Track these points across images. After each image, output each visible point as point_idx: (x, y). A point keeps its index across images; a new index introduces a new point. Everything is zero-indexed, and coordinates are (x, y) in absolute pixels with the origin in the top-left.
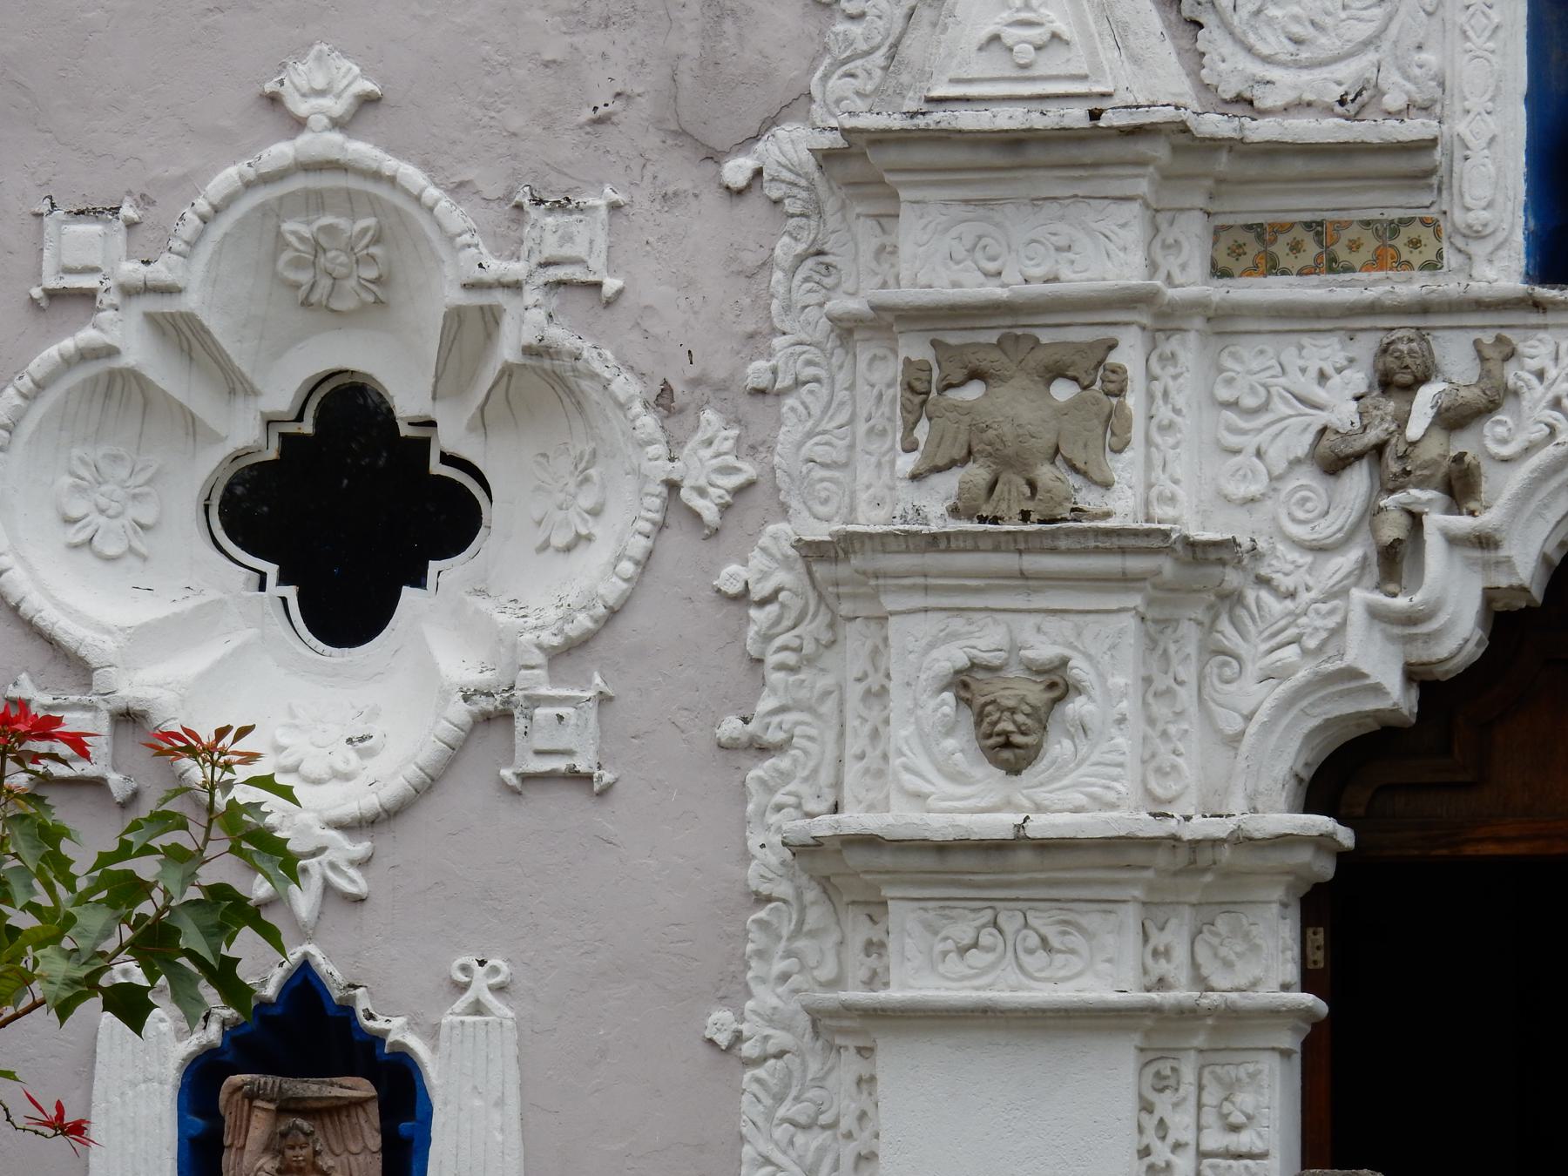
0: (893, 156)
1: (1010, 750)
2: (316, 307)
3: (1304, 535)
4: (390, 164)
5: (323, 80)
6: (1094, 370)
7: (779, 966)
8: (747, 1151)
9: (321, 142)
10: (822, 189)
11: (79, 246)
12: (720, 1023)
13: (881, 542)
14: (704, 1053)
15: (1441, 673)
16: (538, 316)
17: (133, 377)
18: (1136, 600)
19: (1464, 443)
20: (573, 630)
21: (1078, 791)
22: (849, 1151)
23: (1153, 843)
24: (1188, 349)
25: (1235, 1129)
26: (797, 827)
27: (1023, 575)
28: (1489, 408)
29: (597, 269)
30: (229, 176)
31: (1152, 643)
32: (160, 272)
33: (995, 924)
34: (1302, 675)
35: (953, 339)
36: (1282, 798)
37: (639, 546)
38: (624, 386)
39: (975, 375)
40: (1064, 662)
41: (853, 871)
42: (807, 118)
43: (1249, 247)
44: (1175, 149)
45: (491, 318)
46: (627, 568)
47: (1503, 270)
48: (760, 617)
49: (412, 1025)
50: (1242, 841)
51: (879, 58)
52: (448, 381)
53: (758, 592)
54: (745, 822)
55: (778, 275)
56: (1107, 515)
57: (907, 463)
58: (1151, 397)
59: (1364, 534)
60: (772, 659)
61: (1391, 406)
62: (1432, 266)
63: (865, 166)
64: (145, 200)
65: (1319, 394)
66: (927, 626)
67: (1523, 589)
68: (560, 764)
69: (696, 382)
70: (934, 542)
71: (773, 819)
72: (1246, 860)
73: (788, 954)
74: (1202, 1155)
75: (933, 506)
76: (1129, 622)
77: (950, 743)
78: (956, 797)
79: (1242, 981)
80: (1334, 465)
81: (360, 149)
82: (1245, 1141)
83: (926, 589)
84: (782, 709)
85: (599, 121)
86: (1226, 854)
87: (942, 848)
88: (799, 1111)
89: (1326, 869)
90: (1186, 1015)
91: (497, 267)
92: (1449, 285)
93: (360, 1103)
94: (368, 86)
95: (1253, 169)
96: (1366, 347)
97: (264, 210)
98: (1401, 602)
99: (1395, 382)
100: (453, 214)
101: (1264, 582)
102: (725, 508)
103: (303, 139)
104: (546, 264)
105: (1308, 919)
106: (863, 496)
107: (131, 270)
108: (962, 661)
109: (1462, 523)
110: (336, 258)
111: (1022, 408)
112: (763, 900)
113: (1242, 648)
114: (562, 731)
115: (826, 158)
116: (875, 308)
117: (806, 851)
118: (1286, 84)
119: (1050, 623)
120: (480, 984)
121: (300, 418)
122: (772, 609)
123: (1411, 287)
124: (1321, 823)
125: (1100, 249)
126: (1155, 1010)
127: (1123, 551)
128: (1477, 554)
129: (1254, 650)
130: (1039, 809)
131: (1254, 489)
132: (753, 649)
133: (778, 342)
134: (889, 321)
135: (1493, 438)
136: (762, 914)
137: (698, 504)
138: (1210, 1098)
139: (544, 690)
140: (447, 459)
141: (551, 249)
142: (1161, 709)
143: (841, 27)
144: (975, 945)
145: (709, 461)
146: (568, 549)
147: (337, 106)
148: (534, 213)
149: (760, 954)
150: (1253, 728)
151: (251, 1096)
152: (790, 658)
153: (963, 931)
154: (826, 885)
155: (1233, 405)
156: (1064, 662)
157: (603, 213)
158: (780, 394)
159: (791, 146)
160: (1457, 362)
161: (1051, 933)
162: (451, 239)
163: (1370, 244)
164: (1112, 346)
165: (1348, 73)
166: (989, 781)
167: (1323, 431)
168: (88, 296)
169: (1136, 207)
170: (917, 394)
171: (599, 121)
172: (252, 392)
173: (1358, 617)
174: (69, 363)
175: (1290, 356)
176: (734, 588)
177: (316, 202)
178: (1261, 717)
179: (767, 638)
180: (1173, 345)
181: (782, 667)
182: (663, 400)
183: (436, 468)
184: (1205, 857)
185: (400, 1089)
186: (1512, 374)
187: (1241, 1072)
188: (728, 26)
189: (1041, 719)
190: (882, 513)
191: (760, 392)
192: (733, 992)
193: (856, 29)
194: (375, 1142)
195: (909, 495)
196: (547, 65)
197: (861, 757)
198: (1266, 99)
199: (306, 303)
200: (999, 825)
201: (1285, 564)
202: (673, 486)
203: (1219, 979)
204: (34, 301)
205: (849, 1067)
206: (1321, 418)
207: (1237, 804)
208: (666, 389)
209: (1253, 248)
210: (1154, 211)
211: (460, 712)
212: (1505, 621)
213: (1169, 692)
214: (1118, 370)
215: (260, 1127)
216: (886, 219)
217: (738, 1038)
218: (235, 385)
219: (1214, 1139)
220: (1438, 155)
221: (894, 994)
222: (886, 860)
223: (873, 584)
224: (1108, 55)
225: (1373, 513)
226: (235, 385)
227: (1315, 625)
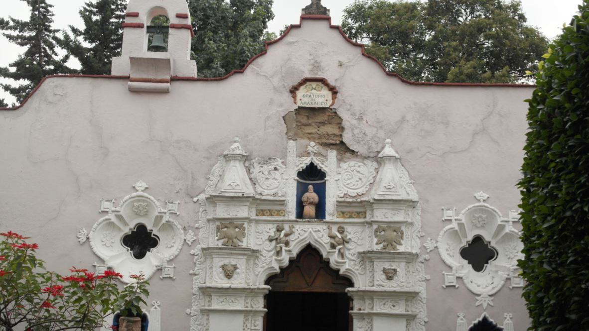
0: (217, 199)
1: (229, 276)
2: (138, 215)
3: (266, 249)
4: (149, 196)
6: (241, 227)
7: (196, 303)
8: (191, 328)
10: (206, 202)
11: (106, 205)
12: (188, 311)
13: (213, 248)
14: (186, 315)
15: (283, 268)
16: (168, 217)
17: (113, 223)
18: (246, 257)
19: (287, 238)
20: (171, 258)
21: (238, 282)
22: (205, 328)
23: (247, 289)
24: (253, 225)
25: (256, 326)
26: (200, 285)
27: (231, 253)
28: (291, 234)
29: (176, 211)
30: (127, 197)
31: (247, 262)
32: (117, 209)
33: (226, 299)
34: (266, 267)
35: (223, 222)
36: (263, 283)
37: (180, 247)
38: (179, 226)
39: (226, 227)
40: (236, 265)
41: (207, 292)
42: (205, 194)
43: (261, 212)
44: (253, 200)
45: (162, 217)
46: (178, 250)
47: (293, 217)
48: (196, 257)
49: (146, 310)
50: (258, 289)
51: (214, 186)
52: (155, 225)
53: (196, 254)
54: (193, 284)
55: (200, 213)
56: (242, 246)
57: (216, 238)
58: (248, 231)
59: (275, 249)
60: (197, 263)
61: (278, 233)
62: (284, 216)
64: (116, 200)
65: (269, 231)
66: (218, 260)
67: (294, 257)
68: (168, 276)
69: (189, 226)
70: (220, 249)
71: (197, 284)
72: (259, 291)
73: (198, 302)
74: (251, 330)
75: (220, 244)
76: (245, 260)
77: (221, 275)
78: (220, 281)
79: (257, 307)
80: (271, 241)
81: (145, 194)
82: (257, 328)
83: (218, 255)
84: (198, 270)
85: (177, 192)
86: (256, 290)
87: (220, 289)
88: (198, 323)
89: (267, 292)
90: (250, 311)
91: (163, 210)
92: (286, 218)
93: (138, 321)
94: (147, 186)
95: (263, 202)
96: (275, 225)
97: (132, 202)
98: (279, 258)
99: (279, 230)
100: (157, 203)
101: (261, 255)
102: (192, 243)
103: (138, 192)
104: (169, 210)
105: (265, 299)
106: (210, 242)
107: (114, 209)
108: (223, 264)
109: (287, 249)
110: (141, 208)
111: (232, 232)
112: (194, 295)
113: (259, 264)
114: (169, 271)
115: (207, 199)
116: (213, 218)
117: (200, 288)
118: (266, 192)
119: (235, 260)
120: (156, 305)
121: (134, 229)
122: (198, 256)
123: (282, 218)
124: (268, 287)
125: (242, 212)
126: (246, 311)
127: (245, 251)
128: (289, 253)
129: (260, 264)
130: (233, 284)
131: (261, 243)
132: (195, 261)
133: (200, 222)
135: (291, 238)
136: (194, 296)
137: (189, 242)
138: (253, 322)
139: (167, 266)
140: (154, 235)
141: (170, 208)
142: (248, 271)
143: (210, 182)
144: (223, 301)
145: (190, 237)
146: (170, 248)
147: (143, 189)
148: (168, 204)
149: (194, 302)
150: (260, 274)
151: (124, 320)
152: (199, 263)
153: (222, 300)
154: (203, 293)
155: (258, 232)
156: (236, 265)
157: (177, 204)
158: (200, 228)
159: (202, 197)
160: (287, 228)
161: (233, 300)
162: (157, 206)
163: (276, 213)
164: (244, 224)
165: (274, 191)
166: (226, 280)
167: (270, 236)
168: (107, 212)
169: (247, 207)
170: (218, 229)
171: (177, 192)
172: (128, 225)
173: (274, 260)
174: (104, 221)
175: (266, 226)
176: (193, 253)
177: (139, 201)
178: (261, 272)
179: (196, 260)
180: (251, 224)
181: (199, 264)
182: (184, 229)
183: (152, 236)
184: (253, 291)
185: (144, 319)
186: (293, 230)
187: (257, 319)
188: (195, 181)
189: (233, 272)
190: (213, 244)
191: (197, 228)
192: (190, 307)
193: (211, 182)
194: (140, 326)
195: (217, 242)
196: (171, 185)
197: (209, 276)
198: (264, 194)
199: (136, 214)
200: (227, 286)
201: (264, 253)
202: (185, 240)
203: (254, 306)
204: (100, 213)
205: (206, 317)
206: (269, 234)
207: (257, 284)
208: (185, 227)
209: (261, 213)
210: (249, 207)
211: (155, 269)
212: (291, 261)
213: (249, 269)
214: (244, 227)
215: (124, 324)
216: (215, 206)
217: (190, 313)
218: (126, 224)
219: (253, 328)
220: (285, 202)
221: (212, 308)
222: (212, 290)
223: (211, 254)
224: (244, 187)
225: (276, 247)
226: (126, 224)
227: (268, 261)
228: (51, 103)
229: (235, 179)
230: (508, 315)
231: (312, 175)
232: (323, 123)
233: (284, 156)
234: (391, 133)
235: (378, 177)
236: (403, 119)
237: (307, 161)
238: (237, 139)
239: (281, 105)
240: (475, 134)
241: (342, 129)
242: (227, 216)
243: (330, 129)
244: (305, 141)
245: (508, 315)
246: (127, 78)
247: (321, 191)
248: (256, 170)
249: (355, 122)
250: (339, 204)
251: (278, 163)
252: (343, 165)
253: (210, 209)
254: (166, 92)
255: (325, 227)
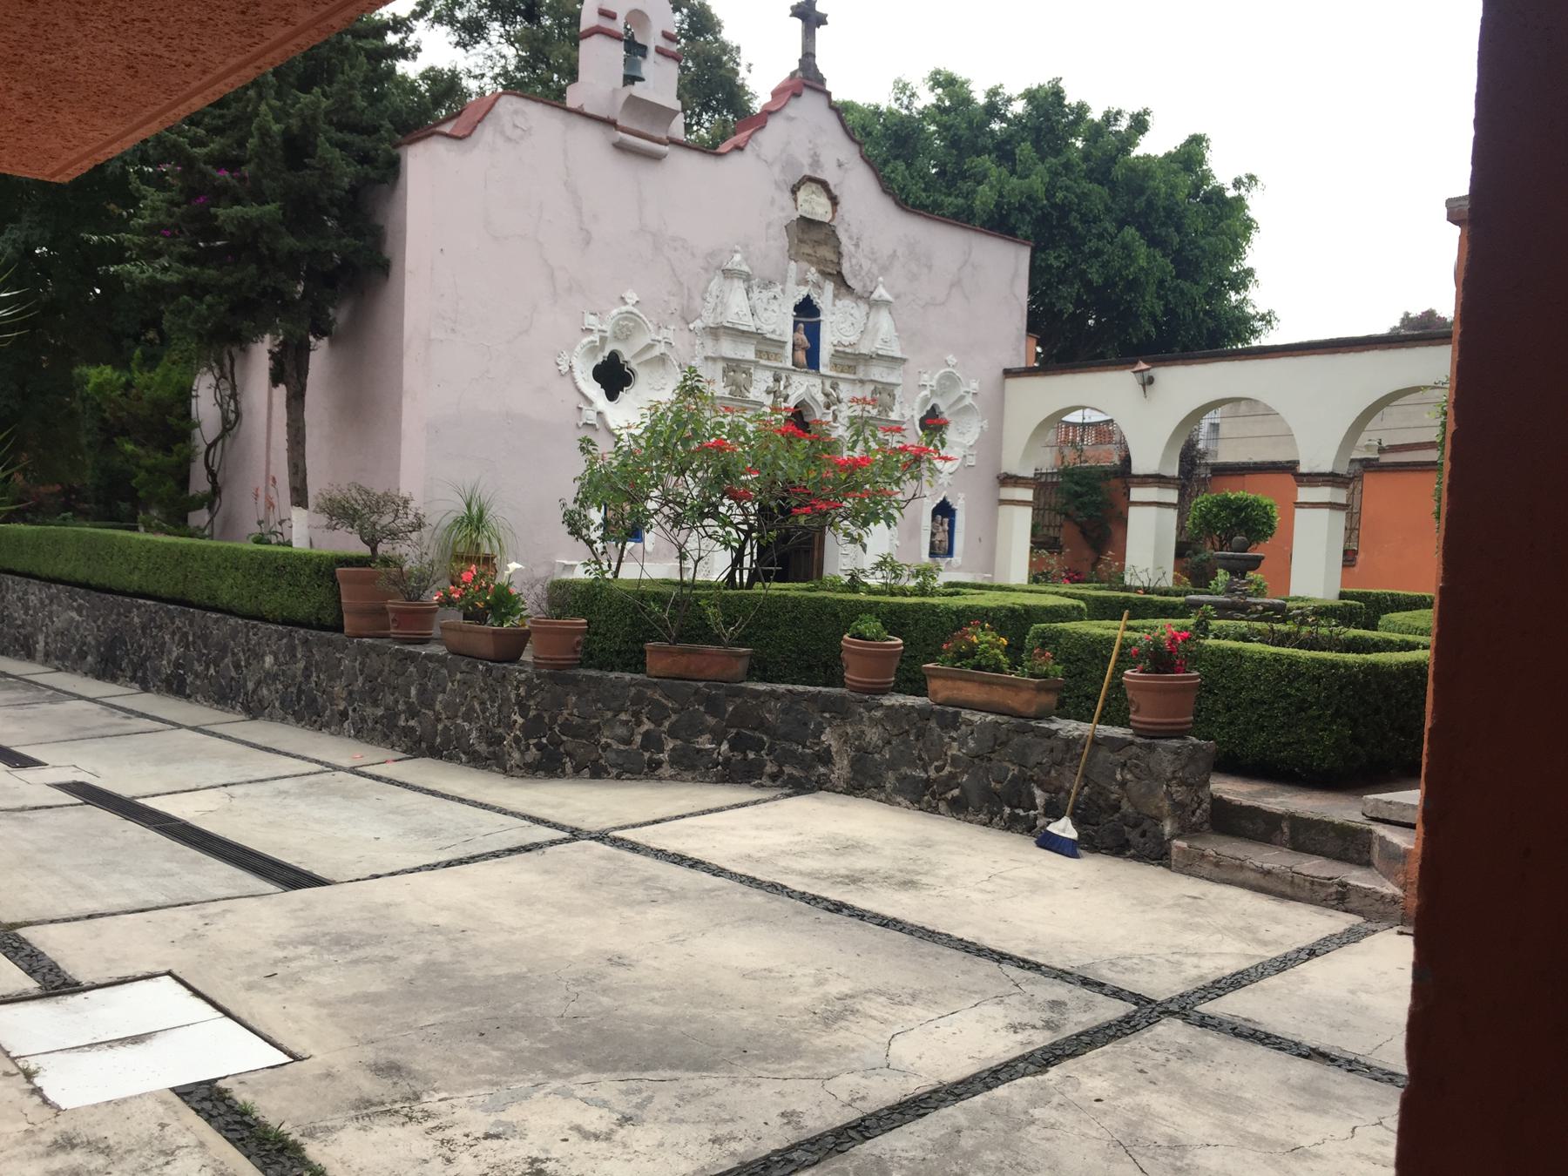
5: (632, 297)
9: (629, 308)
11: (591, 321)
30: (615, 312)
47: (789, 364)
63: (715, 332)
81: (635, 310)
99: (777, 380)
125: (748, 352)
134: (714, 359)
135: (789, 391)
159: (698, 324)
228: (509, 139)
229: (736, 306)
230: (962, 495)
231: (807, 310)
232: (818, 243)
233: (784, 282)
234: (884, 270)
235: (870, 324)
236: (894, 255)
237: (804, 291)
238: (738, 248)
239: (783, 209)
240: (952, 286)
241: (840, 254)
242: (733, 356)
243: (826, 252)
244: (805, 265)
245: (962, 495)
246: (610, 123)
247: (813, 332)
248: (755, 294)
249: (852, 248)
250: (837, 354)
251: (777, 289)
252: (838, 302)
253: (709, 343)
254: (657, 158)
255: (818, 381)
